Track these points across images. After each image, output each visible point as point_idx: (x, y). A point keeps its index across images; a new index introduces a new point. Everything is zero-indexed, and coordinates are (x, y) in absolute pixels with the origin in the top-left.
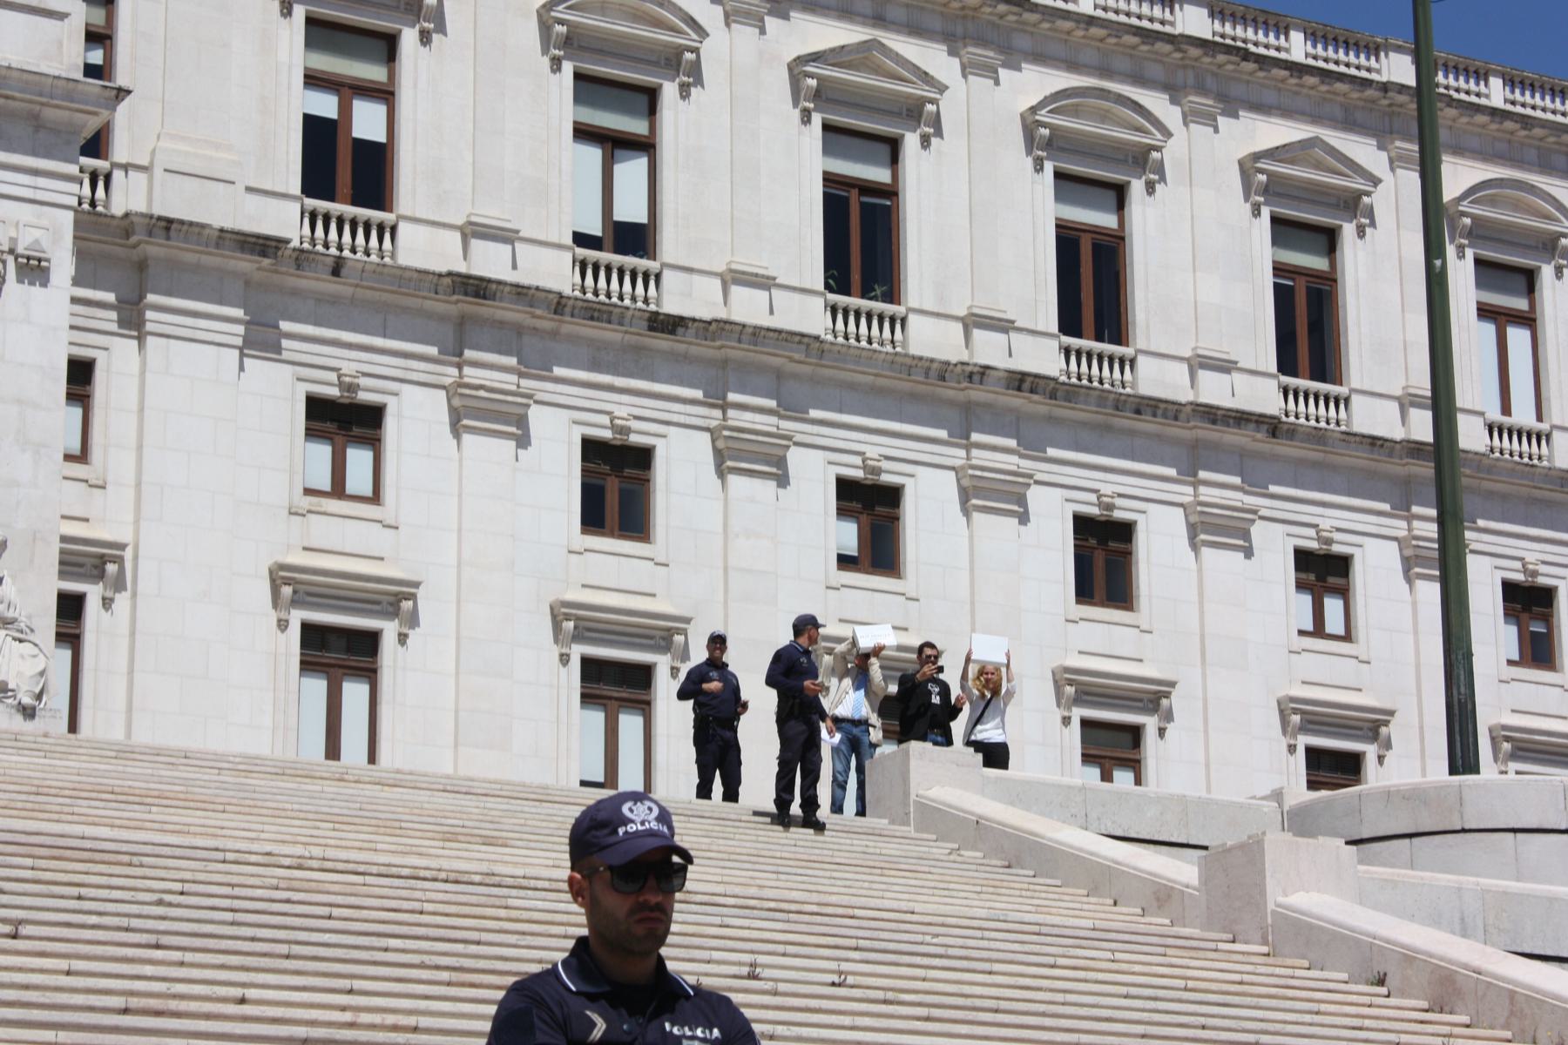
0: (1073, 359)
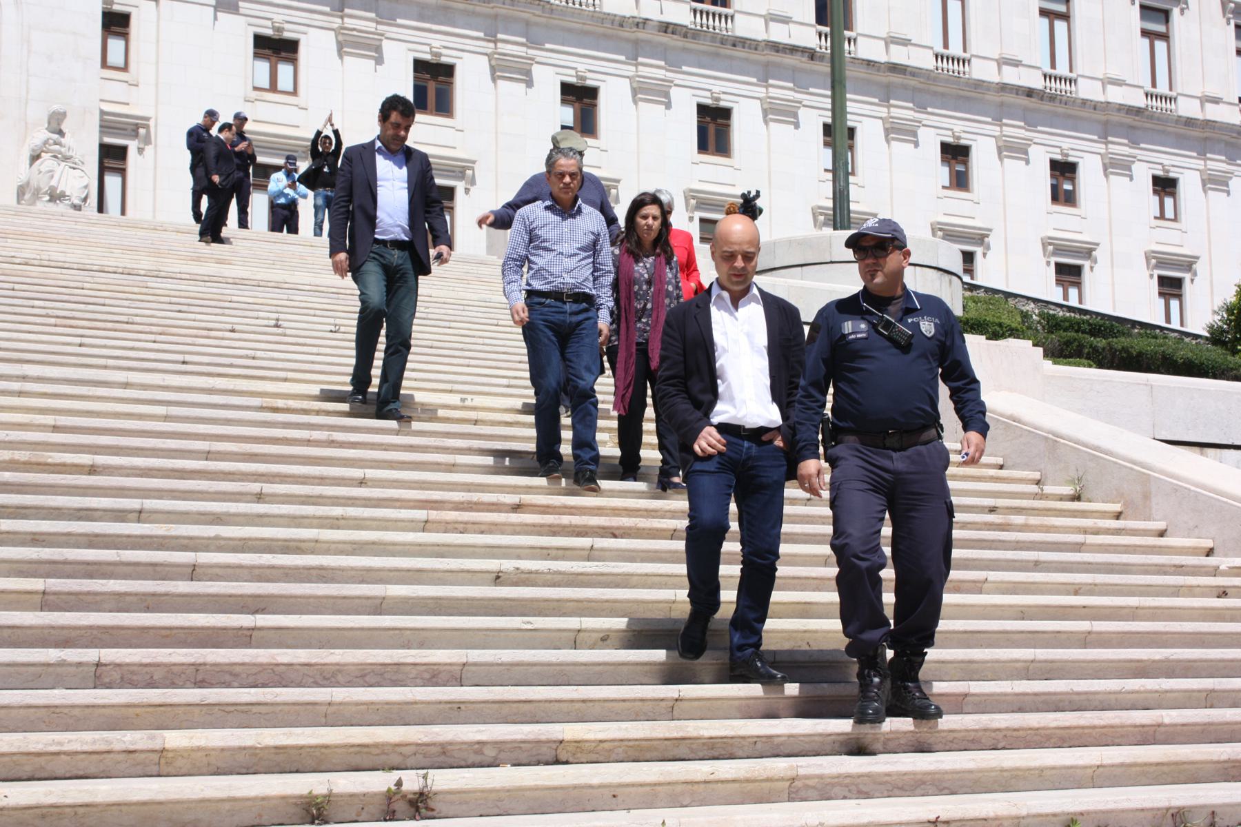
0: (698, 15)
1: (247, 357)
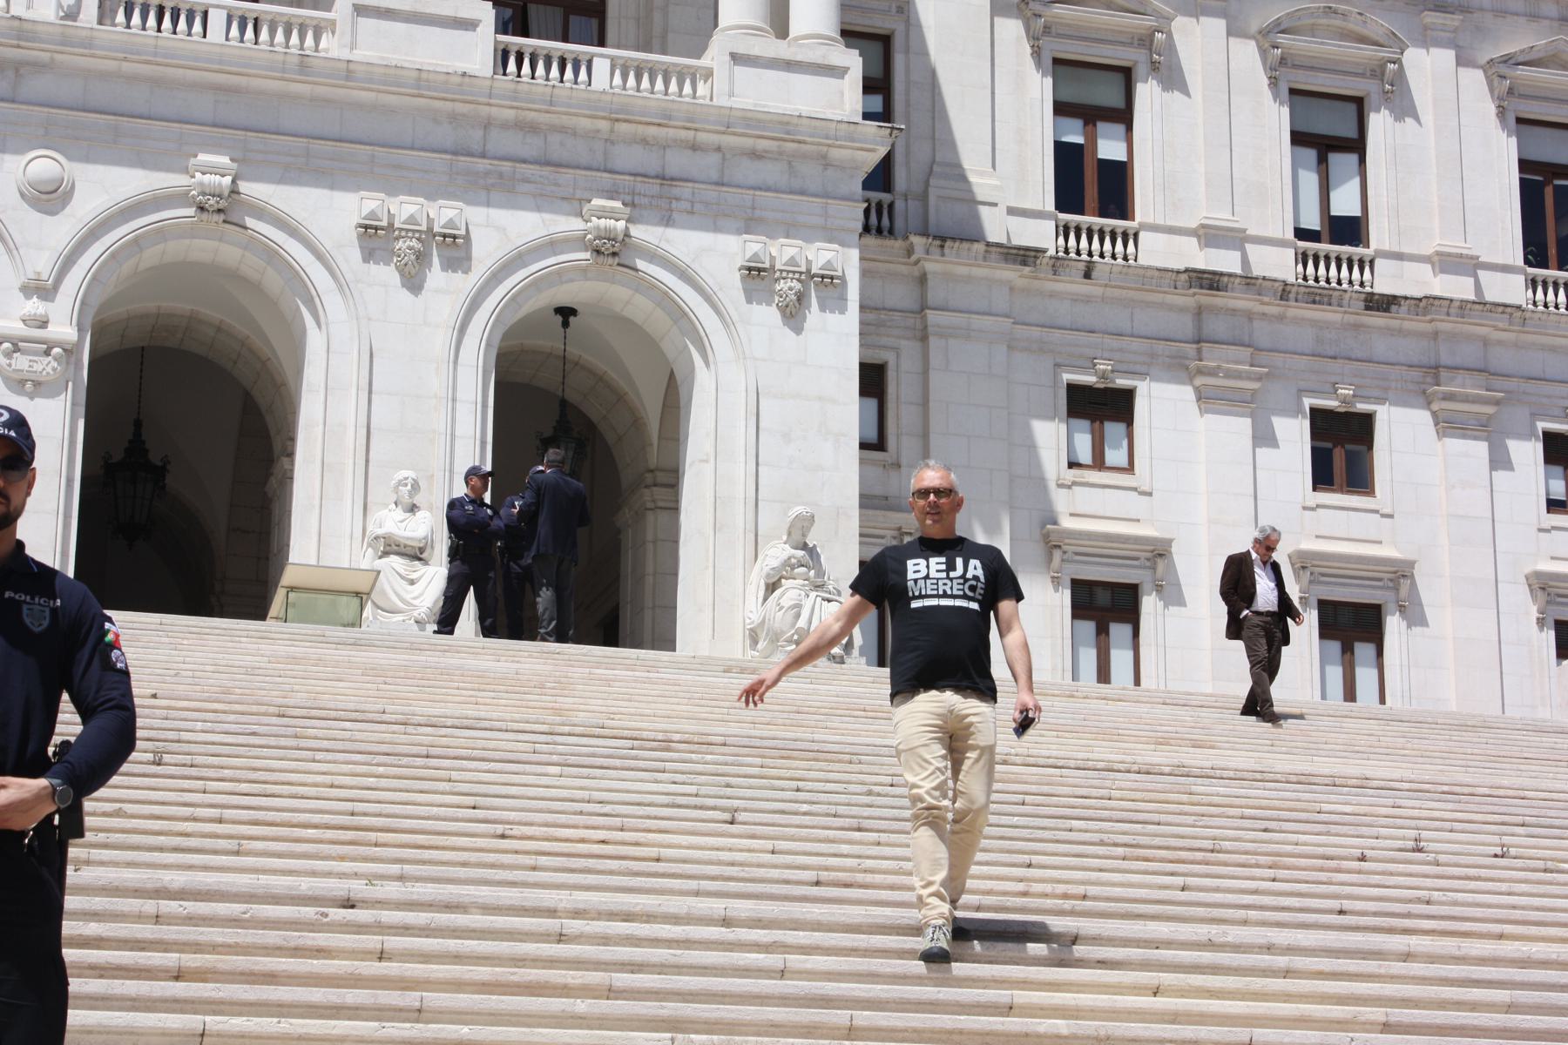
1: (1419, 900)
